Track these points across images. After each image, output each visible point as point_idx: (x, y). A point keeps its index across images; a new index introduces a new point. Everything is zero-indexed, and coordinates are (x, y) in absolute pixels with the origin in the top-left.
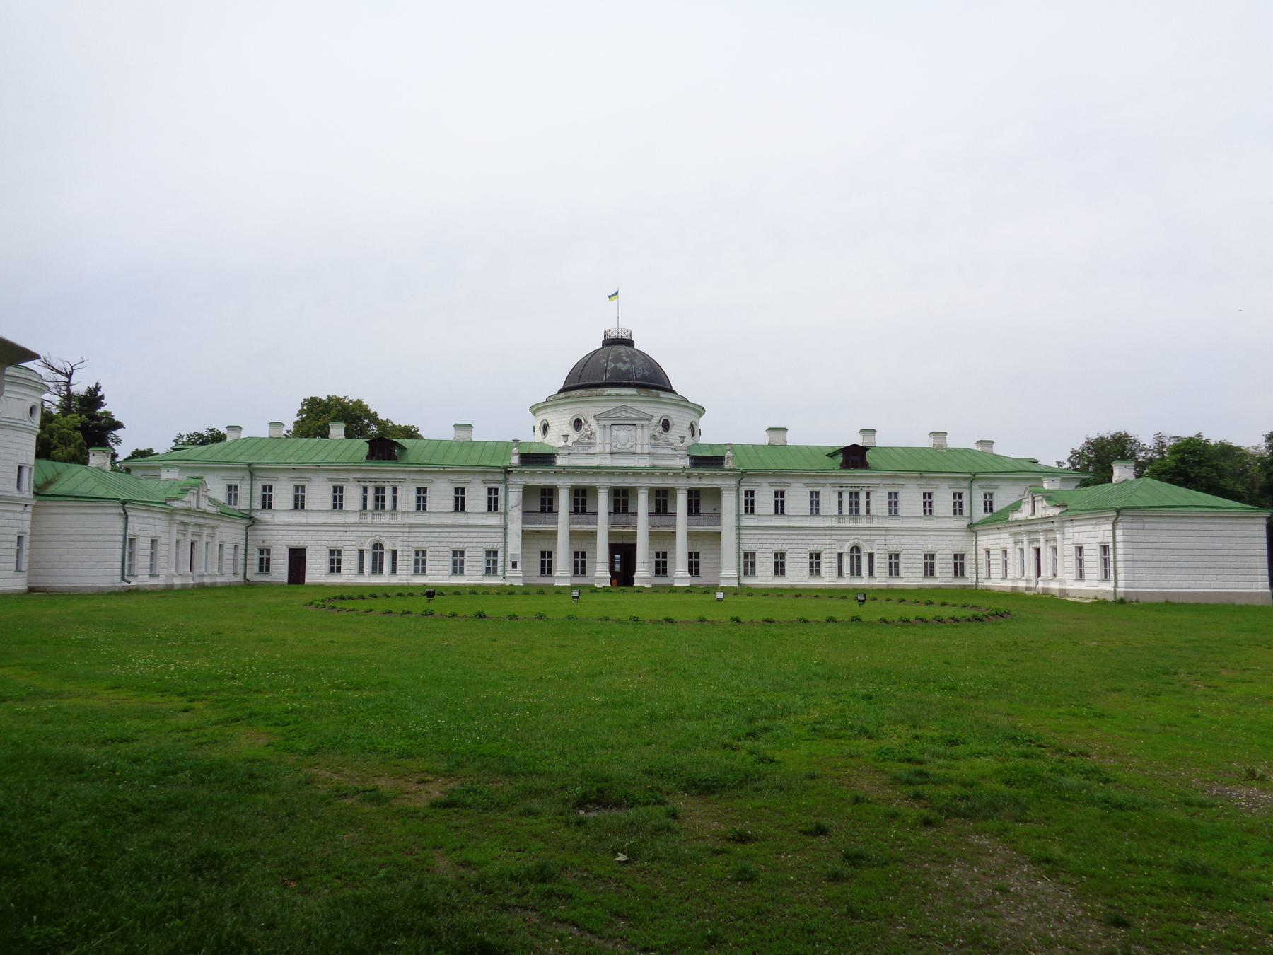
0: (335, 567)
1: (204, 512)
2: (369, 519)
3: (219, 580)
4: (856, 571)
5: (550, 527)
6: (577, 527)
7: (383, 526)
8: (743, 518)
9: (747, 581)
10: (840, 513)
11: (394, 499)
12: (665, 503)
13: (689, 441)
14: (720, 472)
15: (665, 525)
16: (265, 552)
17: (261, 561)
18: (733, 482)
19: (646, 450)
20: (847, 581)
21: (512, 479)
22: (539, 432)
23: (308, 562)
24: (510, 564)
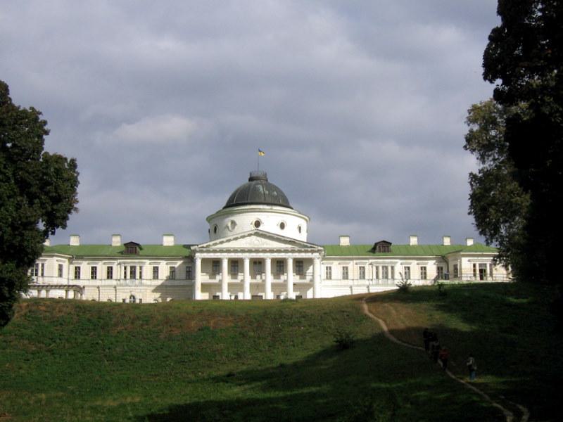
10: (377, 277)
11: (141, 273)
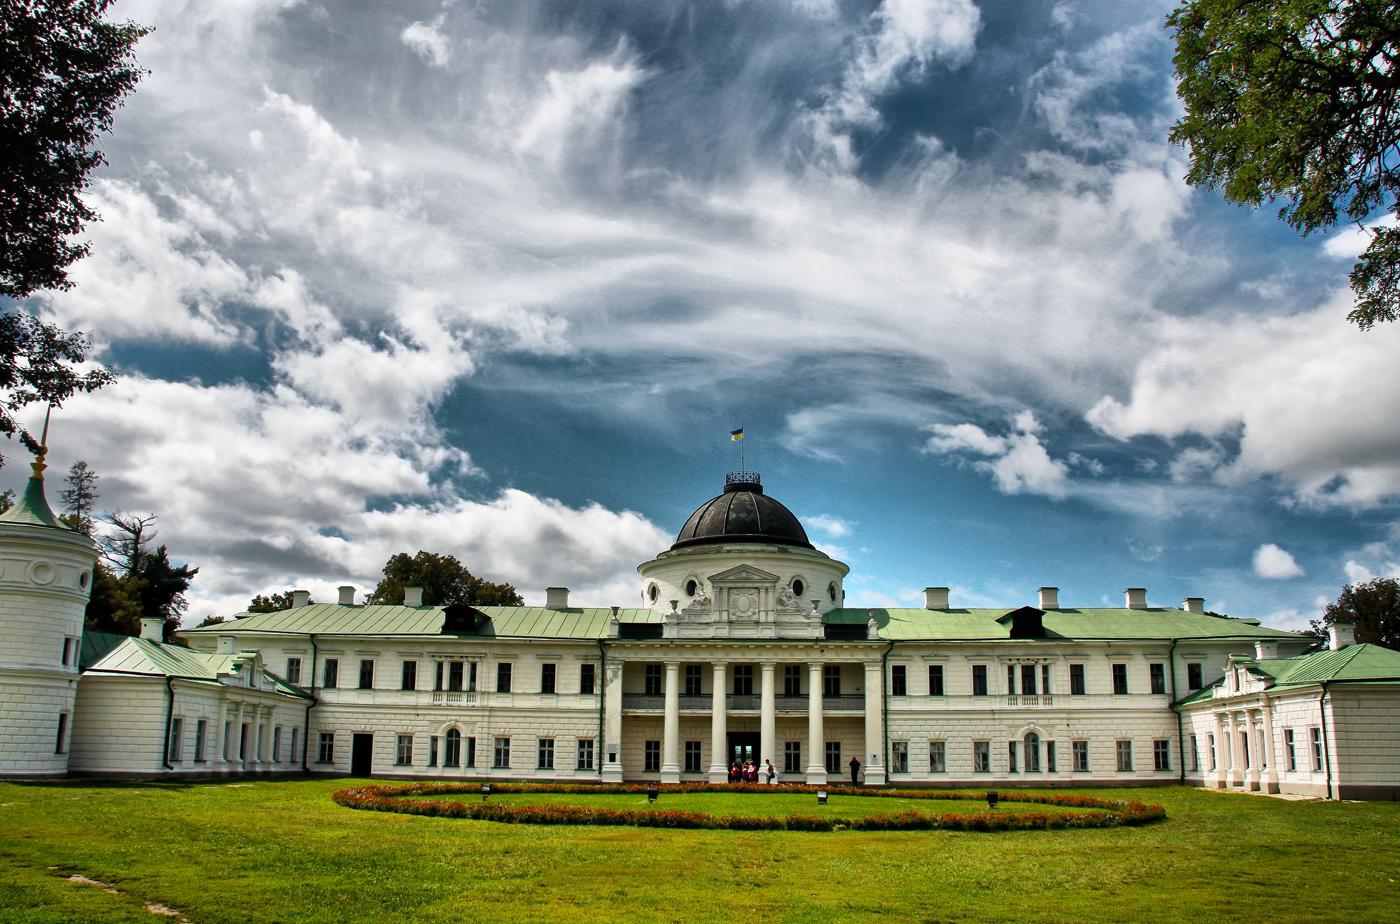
0: (404, 759)
1: (259, 691)
2: (444, 701)
3: (273, 769)
4: (1033, 765)
5: (656, 712)
6: (687, 712)
7: (460, 708)
9: (896, 778)
12: (797, 683)
13: (826, 605)
14: (862, 644)
15: (797, 708)
16: (327, 738)
17: (323, 747)
18: (878, 656)
19: (771, 618)
20: (1021, 776)
21: (610, 654)
22: (647, 597)
23: (374, 750)
24: (607, 757)
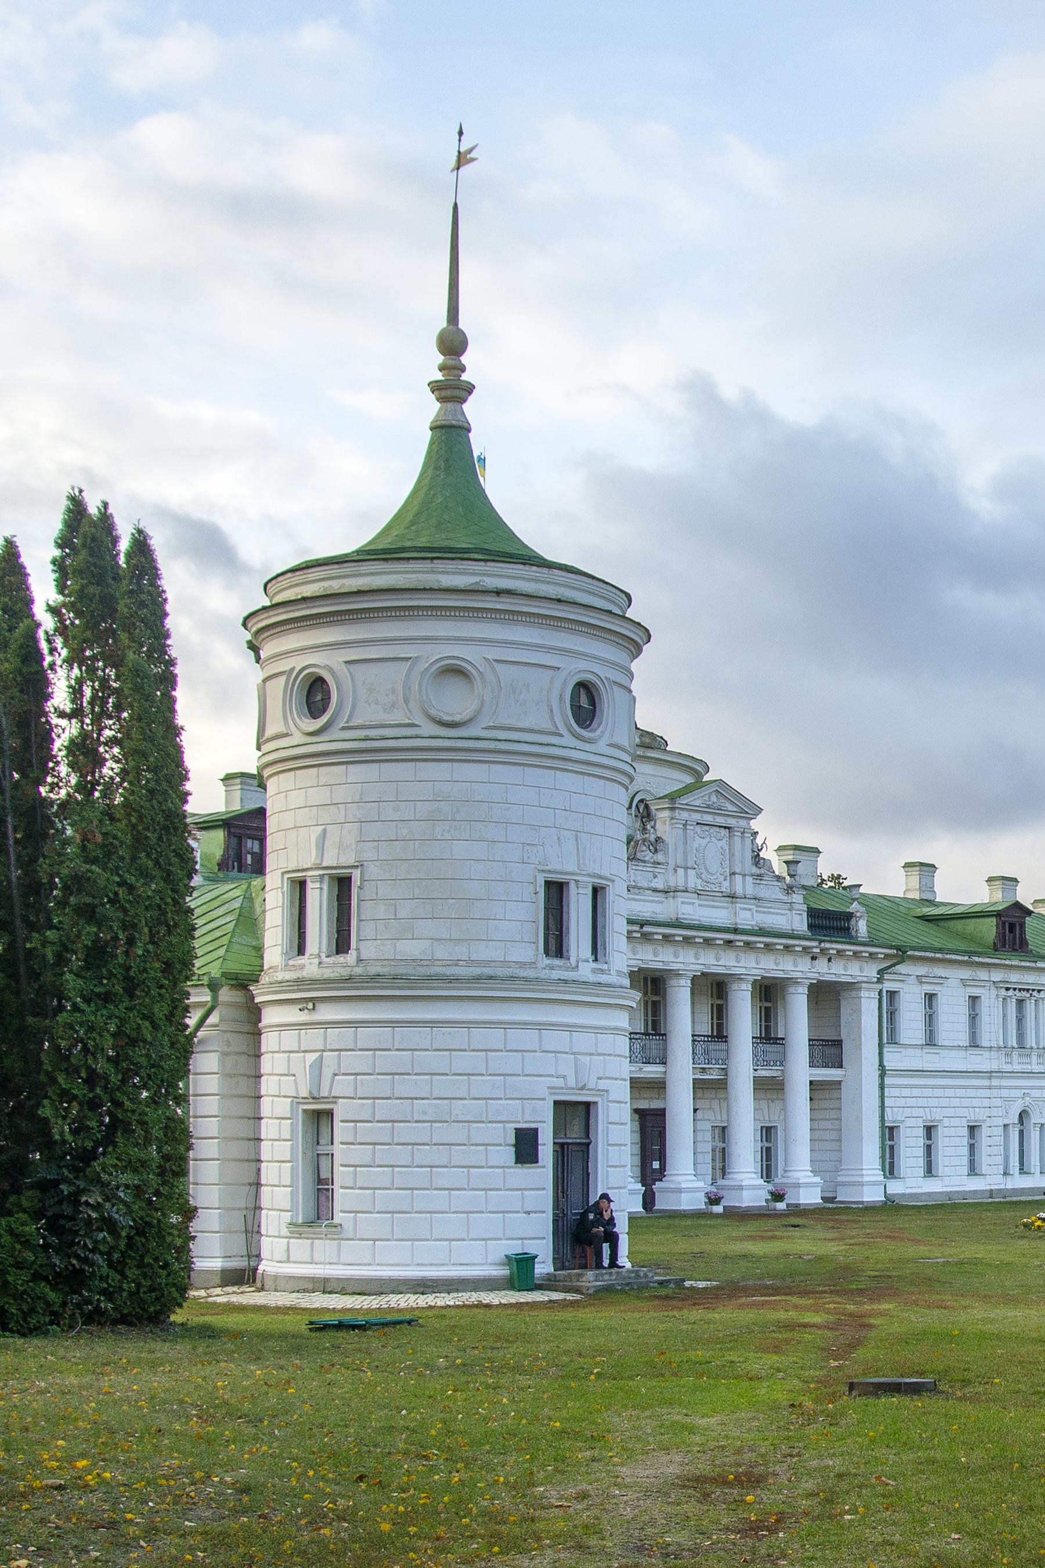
8: (885, 1050)
9: (895, 1188)
18: (871, 971)
